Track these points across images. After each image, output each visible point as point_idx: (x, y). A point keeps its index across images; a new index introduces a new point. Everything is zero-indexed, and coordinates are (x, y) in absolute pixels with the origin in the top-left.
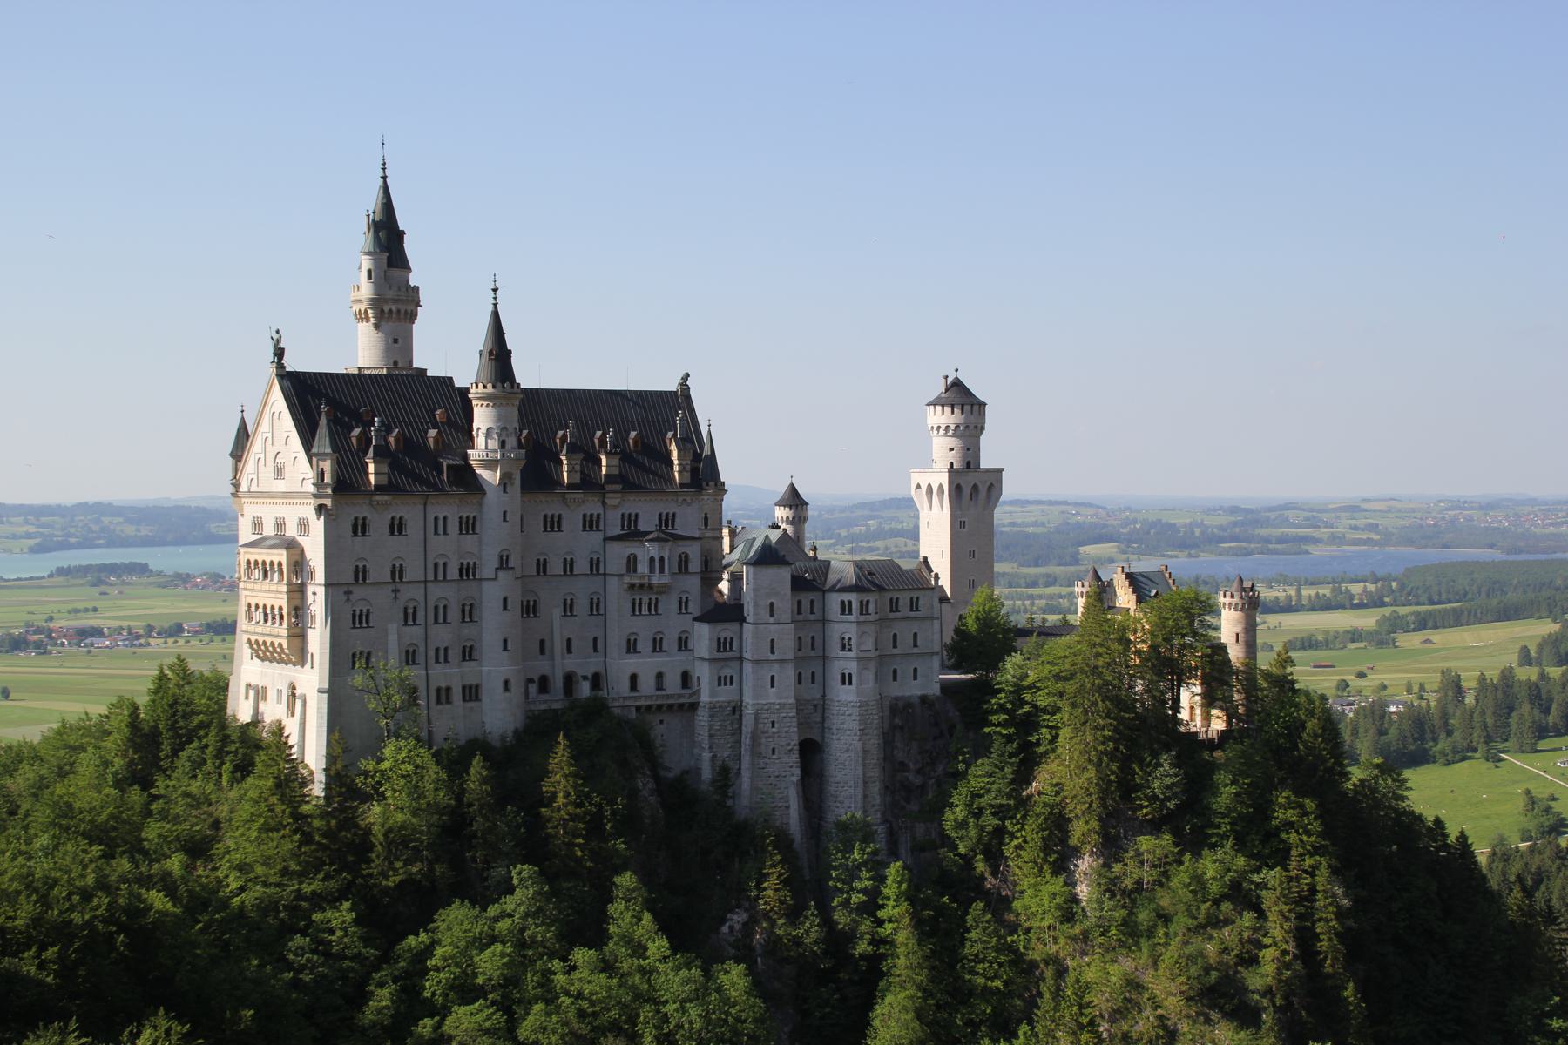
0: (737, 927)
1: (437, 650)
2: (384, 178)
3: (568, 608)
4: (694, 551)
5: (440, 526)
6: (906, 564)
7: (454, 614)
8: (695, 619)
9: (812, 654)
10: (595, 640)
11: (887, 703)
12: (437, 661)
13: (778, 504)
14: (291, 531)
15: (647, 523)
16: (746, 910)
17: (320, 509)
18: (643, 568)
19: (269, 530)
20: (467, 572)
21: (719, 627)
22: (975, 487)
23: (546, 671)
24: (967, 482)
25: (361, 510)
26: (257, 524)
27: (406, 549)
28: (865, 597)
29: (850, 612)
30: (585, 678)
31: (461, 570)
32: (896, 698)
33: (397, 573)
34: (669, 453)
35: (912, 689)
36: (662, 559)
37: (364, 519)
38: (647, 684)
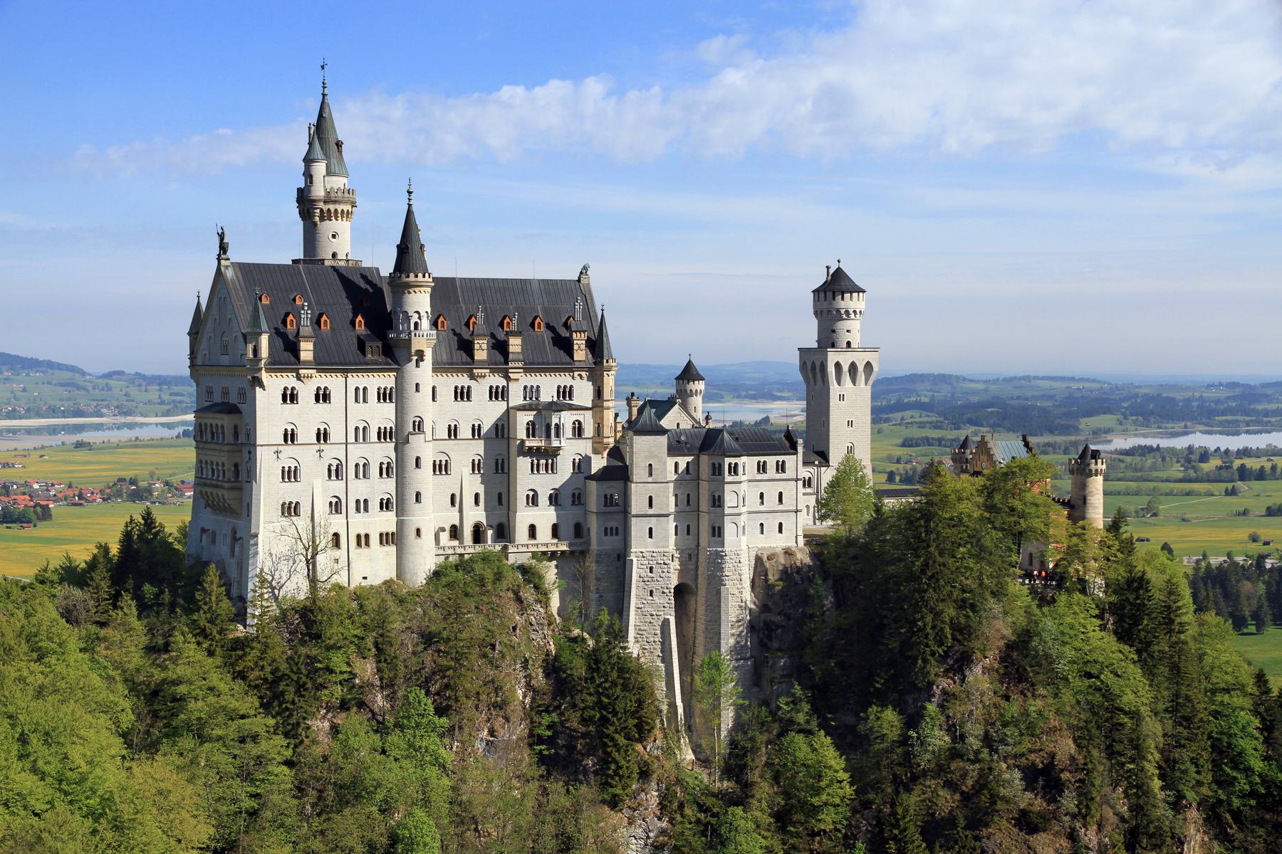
1: (358, 502)
2: (324, 95)
4: (587, 420)
5: (361, 395)
7: (374, 470)
10: (500, 495)
11: (753, 554)
12: (358, 510)
14: (233, 399)
15: (548, 395)
19: (218, 398)
20: (383, 435)
21: (606, 484)
22: (853, 367)
23: (457, 523)
24: (846, 359)
25: (289, 380)
26: (210, 392)
28: (733, 460)
31: (379, 433)
32: (763, 549)
33: (323, 436)
35: (776, 542)
37: (293, 389)
38: (544, 535)
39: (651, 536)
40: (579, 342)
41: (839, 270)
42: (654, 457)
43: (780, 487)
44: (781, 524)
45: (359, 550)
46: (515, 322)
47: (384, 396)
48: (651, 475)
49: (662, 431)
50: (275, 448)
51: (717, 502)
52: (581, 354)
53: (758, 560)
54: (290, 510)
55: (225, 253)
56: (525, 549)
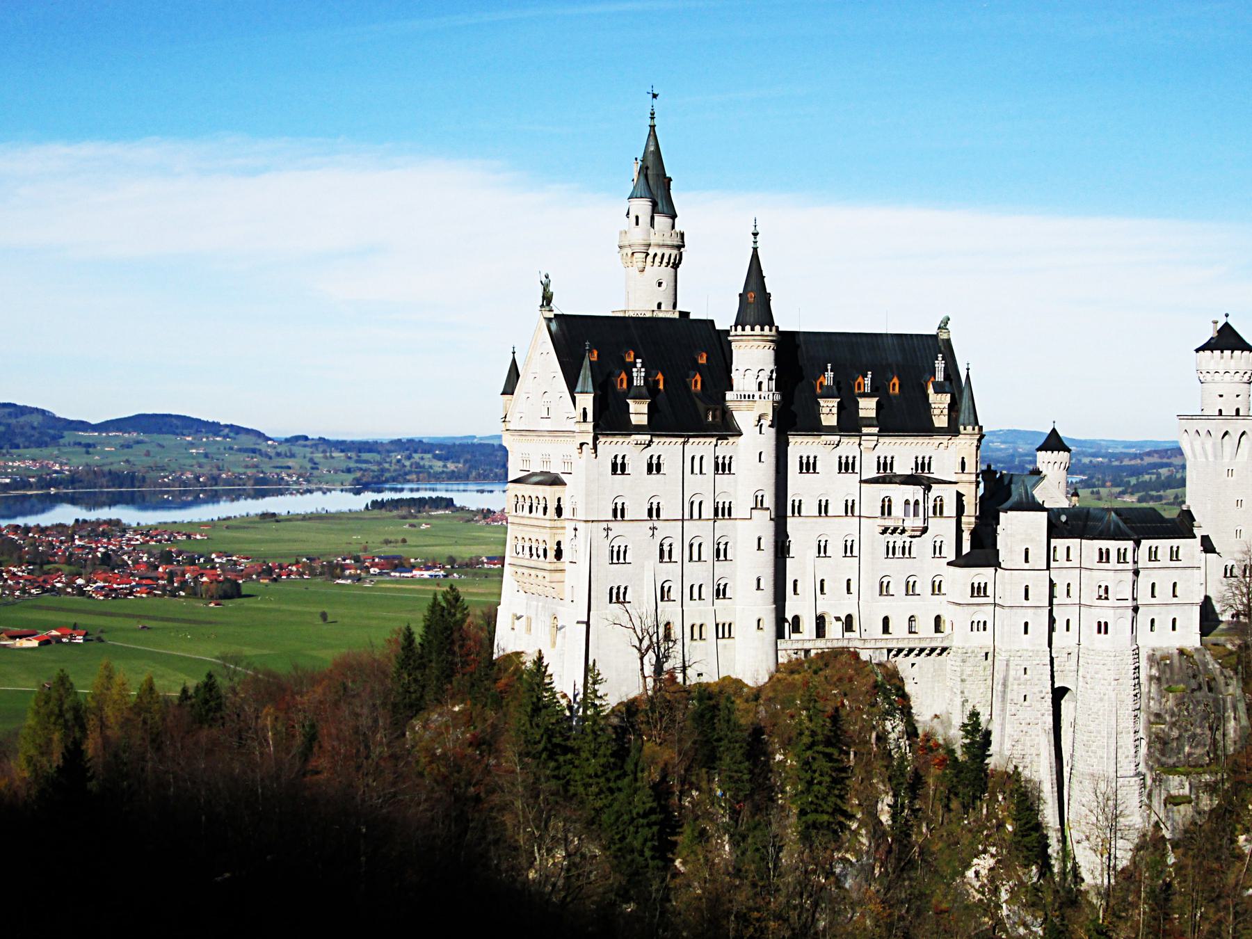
0: (984, 872)
2: (653, 127)
3: (822, 550)
5: (696, 465)
6: (1171, 513)
7: (708, 553)
8: (949, 564)
9: (1068, 601)
10: (849, 580)
13: (1039, 449)
15: (903, 467)
16: (992, 856)
17: (582, 444)
18: (898, 510)
27: (665, 489)
29: (1108, 561)
30: (838, 619)
31: (716, 510)
33: (654, 512)
34: (927, 397)
36: (917, 503)
39: (1026, 632)
40: (939, 403)
41: (1227, 324)
42: (1032, 540)
43: (1174, 576)
44: (1174, 620)
45: (694, 643)
46: (868, 381)
47: (722, 467)
48: (1027, 560)
49: (1040, 508)
50: (605, 525)
51: (1105, 593)
52: (941, 421)
53: (1151, 659)
54: (618, 596)
55: (548, 304)
56: (879, 645)
